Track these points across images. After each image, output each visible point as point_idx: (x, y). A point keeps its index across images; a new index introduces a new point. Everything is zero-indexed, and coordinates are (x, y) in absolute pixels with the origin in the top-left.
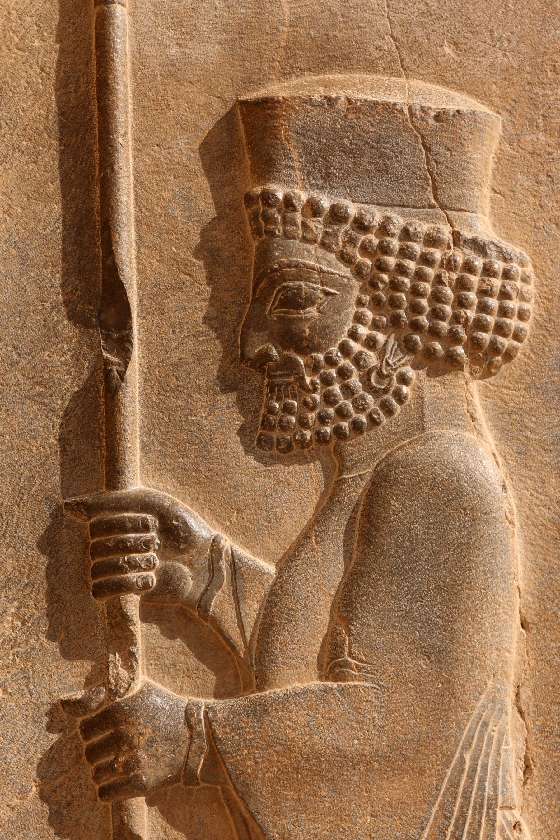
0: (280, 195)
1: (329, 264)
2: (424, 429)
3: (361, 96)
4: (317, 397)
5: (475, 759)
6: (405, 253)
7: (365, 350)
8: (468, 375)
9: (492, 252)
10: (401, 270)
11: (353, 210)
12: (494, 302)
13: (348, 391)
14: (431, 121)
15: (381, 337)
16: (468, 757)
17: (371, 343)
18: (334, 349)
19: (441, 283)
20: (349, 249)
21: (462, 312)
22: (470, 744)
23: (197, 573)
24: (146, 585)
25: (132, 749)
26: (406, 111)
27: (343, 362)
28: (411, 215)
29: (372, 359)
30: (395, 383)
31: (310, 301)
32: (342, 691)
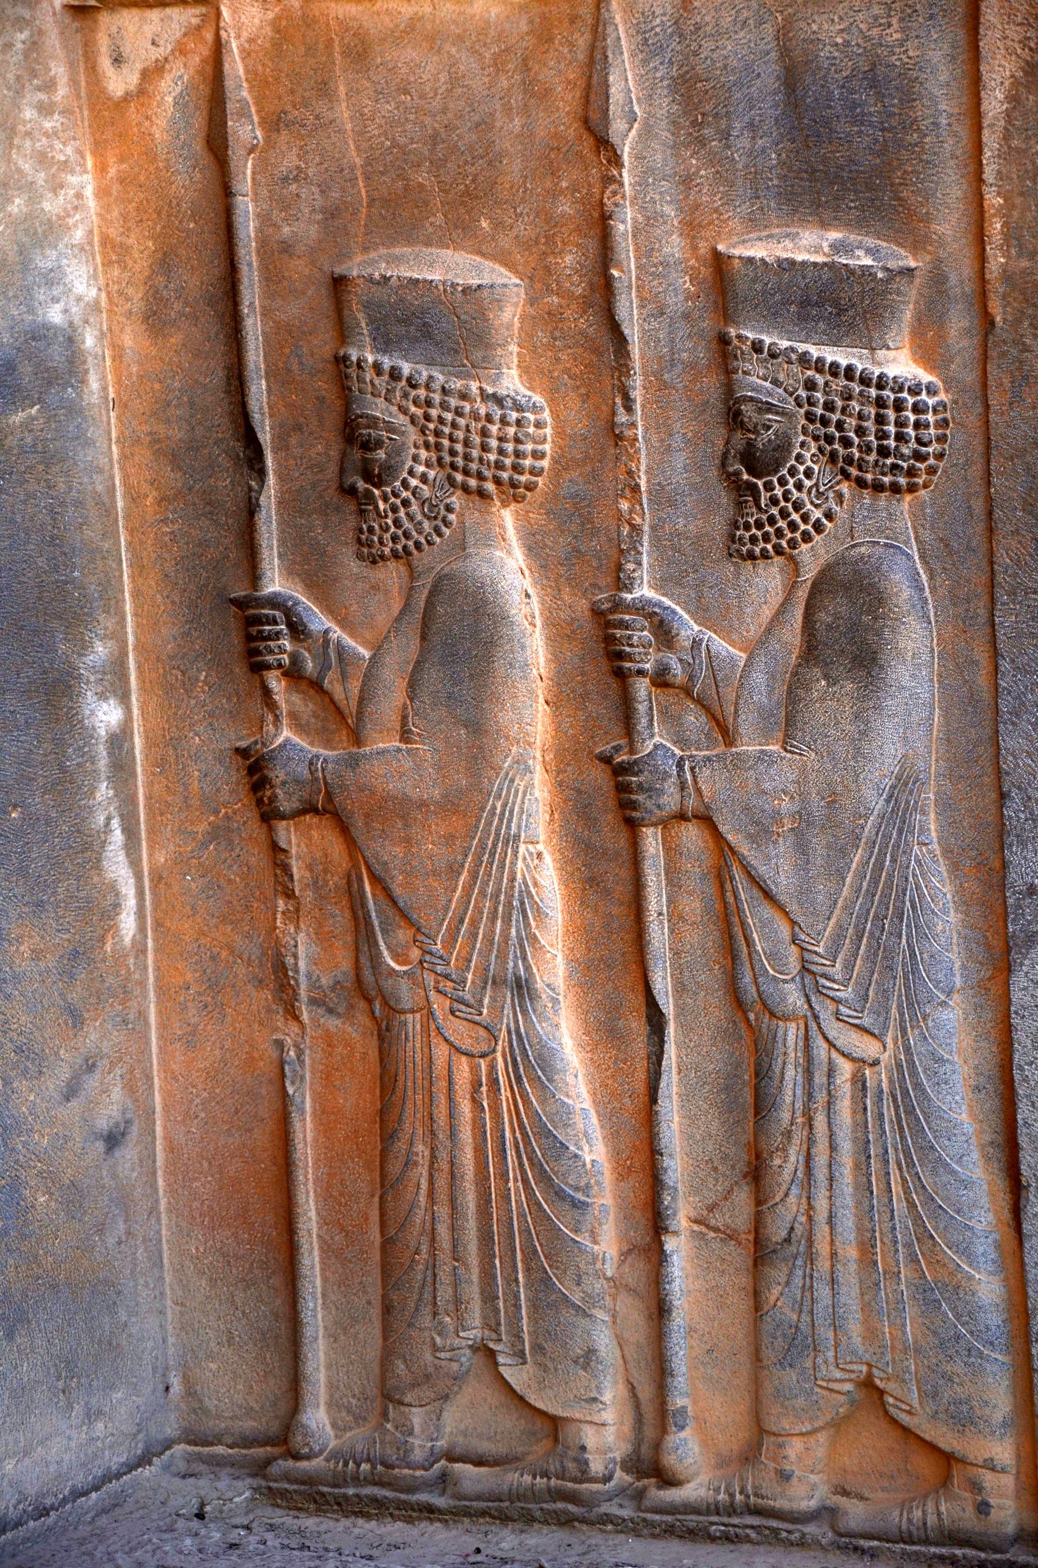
0: (354, 358)
1: (391, 414)
2: (464, 549)
3: (408, 274)
4: (389, 521)
5: (504, 805)
6: (444, 406)
7: (421, 485)
8: (498, 504)
9: (509, 403)
10: (441, 420)
11: (406, 368)
12: (510, 447)
13: (410, 517)
14: (459, 295)
15: (432, 474)
16: (499, 805)
17: (424, 479)
18: (398, 484)
19: (468, 431)
20: (404, 403)
21: (485, 456)
22: (500, 795)
23: (314, 658)
24: (280, 666)
25: (272, 787)
26: (441, 288)
27: (405, 494)
28: (450, 374)
29: (426, 491)
30: (443, 512)
31: (379, 444)
32: (408, 751)
